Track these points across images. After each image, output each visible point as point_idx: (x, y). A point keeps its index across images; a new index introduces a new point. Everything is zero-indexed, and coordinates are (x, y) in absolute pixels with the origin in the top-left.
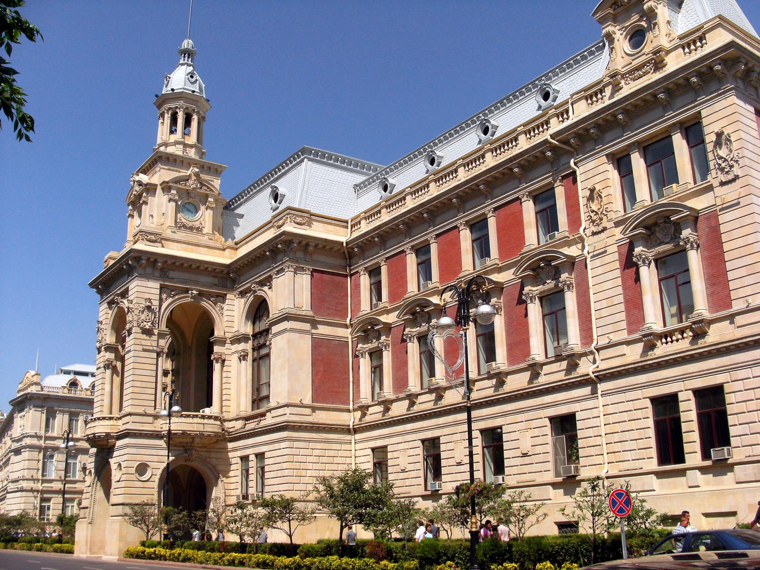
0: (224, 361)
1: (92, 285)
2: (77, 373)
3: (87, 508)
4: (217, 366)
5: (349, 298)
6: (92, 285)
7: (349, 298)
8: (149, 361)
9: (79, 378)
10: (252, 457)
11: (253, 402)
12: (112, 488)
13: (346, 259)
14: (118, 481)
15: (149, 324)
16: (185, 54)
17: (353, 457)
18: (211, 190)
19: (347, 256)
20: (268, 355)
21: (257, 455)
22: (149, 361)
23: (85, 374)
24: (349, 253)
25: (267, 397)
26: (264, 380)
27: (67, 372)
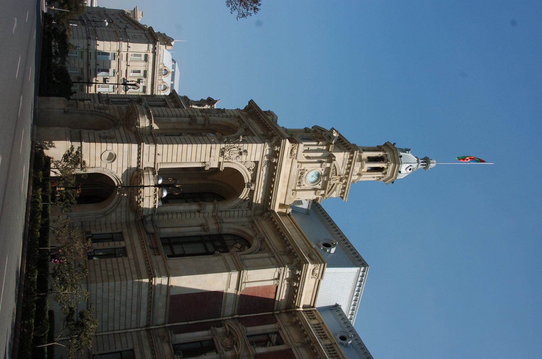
0: (199, 211)
1: (251, 103)
2: (173, 73)
3: (77, 107)
4: (194, 207)
5: (255, 315)
6: (251, 103)
7: (255, 315)
8: (198, 157)
9: (170, 75)
10: (123, 244)
11: (168, 239)
12: (95, 131)
13: (285, 309)
14: (100, 137)
15: (228, 155)
16: (425, 162)
17: (125, 331)
18: (329, 192)
19: (288, 310)
20: (207, 253)
21: (124, 248)
22: (198, 157)
23: (173, 79)
24: (291, 312)
25: (173, 255)
26: (188, 249)
27: (174, 67)
